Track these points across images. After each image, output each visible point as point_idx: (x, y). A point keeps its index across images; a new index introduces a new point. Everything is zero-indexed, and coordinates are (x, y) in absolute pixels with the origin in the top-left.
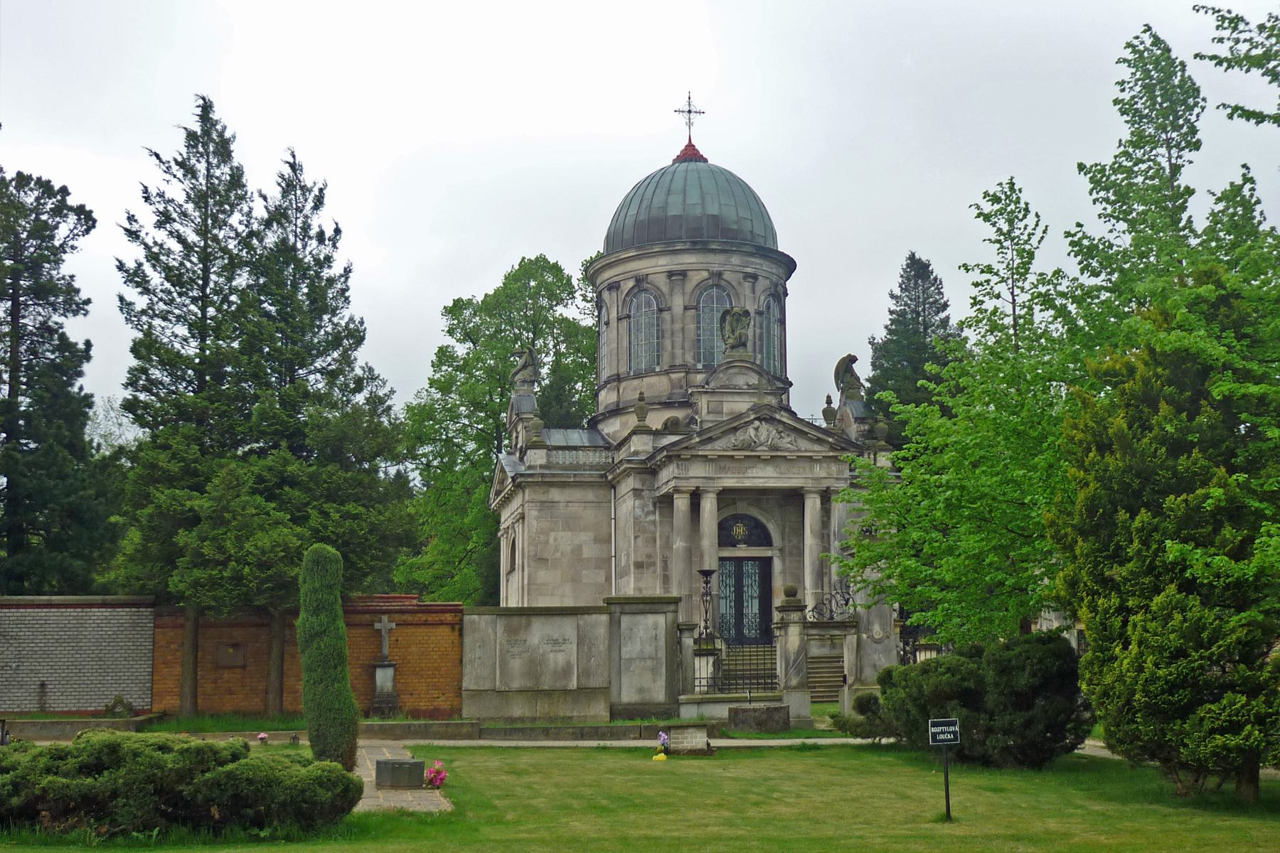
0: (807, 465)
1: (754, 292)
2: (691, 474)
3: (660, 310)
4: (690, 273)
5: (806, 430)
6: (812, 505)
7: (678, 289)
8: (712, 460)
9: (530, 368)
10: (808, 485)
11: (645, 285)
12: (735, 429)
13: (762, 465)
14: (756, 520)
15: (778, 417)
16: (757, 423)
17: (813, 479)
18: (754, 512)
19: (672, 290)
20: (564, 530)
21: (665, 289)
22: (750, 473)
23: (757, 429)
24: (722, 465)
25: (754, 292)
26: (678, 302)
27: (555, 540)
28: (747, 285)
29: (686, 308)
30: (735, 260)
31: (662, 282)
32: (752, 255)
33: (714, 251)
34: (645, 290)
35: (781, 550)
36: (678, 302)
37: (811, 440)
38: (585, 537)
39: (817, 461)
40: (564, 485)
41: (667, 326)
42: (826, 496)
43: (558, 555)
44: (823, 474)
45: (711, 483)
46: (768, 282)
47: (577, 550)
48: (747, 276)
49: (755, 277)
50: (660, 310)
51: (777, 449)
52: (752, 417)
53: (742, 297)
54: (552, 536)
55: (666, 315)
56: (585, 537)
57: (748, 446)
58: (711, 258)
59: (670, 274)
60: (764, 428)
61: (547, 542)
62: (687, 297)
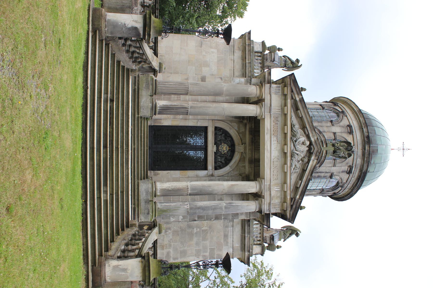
0: (279, 181)
1: (342, 172)
2: (273, 96)
3: (331, 121)
4: (351, 136)
5: (305, 179)
6: (251, 187)
7: (343, 130)
8: (282, 110)
9: (292, 65)
10: (266, 182)
11: (341, 115)
12: (303, 128)
13: (279, 148)
14: (230, 160)
15: (313, 158)
16: (308, 143)
17: (270, 185)
18: (237, 157)
19: (342, 127)
20: (218, 57)
21: (341, 124)
22: (274, 139)
23: (303, 143)
24: (280, 119)
25: (342, 172)
26: (336, 129)
27: (213, 52)
28: (346, 168)
29: (334, 133)
30: (359, 161)
31: (345, 122)
32: (361, 170)
33: (364, 148)
34: (338, 116)
35: (212, 175)
36: (336, 129)
37: (296, 183)
38: (214, 68)
39: (282, 187)
40: (244, 58)
41: (324, 124)
42: (257, 196)
43: (204, 53)
44: (273, 193)
45: (267, 110)
46: (345, 181)
47: (206, 64)
48: (351, 167)
49: (349, 172)
50: (331, 121)
51: (292, 156)
52: (312, 139)
53: (340, 165)
54: (215, 51)
55: (329, 124)
56: (214, 68)
57: (294, 135)
58: (360, 147)
59: (350, 126)
60: (305, 149)
61: (211, 47)
62: (340, 134)
